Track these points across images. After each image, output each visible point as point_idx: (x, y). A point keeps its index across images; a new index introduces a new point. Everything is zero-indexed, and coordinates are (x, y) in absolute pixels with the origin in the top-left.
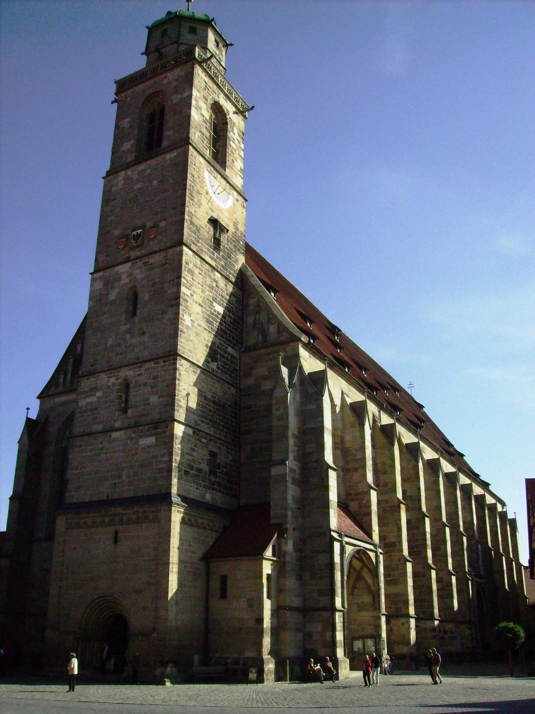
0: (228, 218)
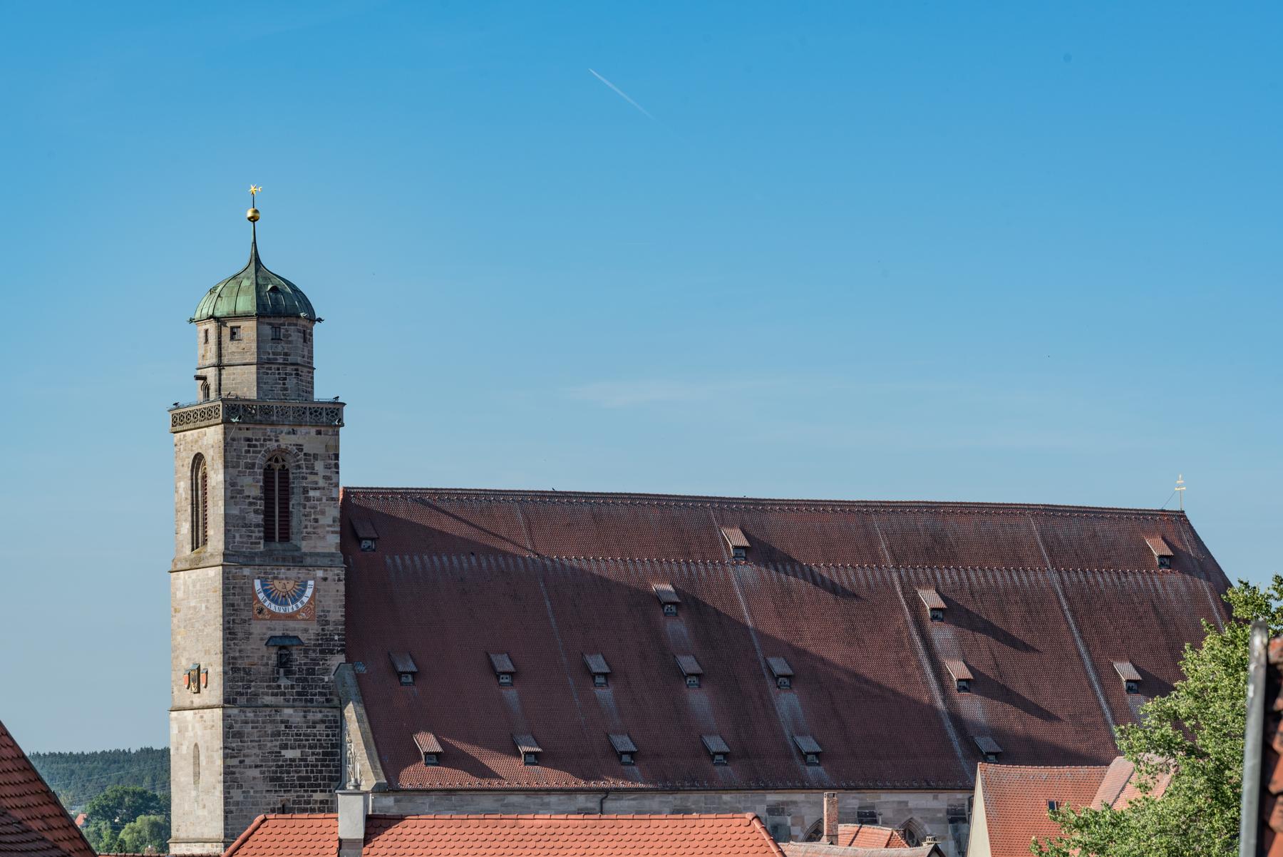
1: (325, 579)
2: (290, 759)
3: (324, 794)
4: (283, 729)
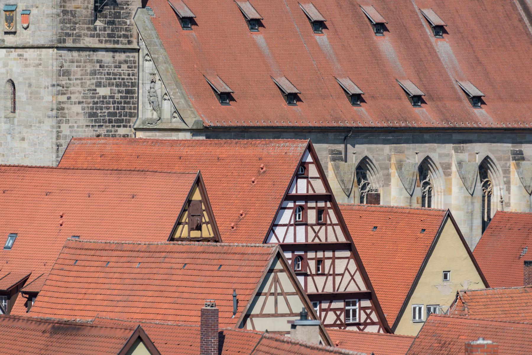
2: (103, 96)
3: (125, 129)
4: (98, 68)
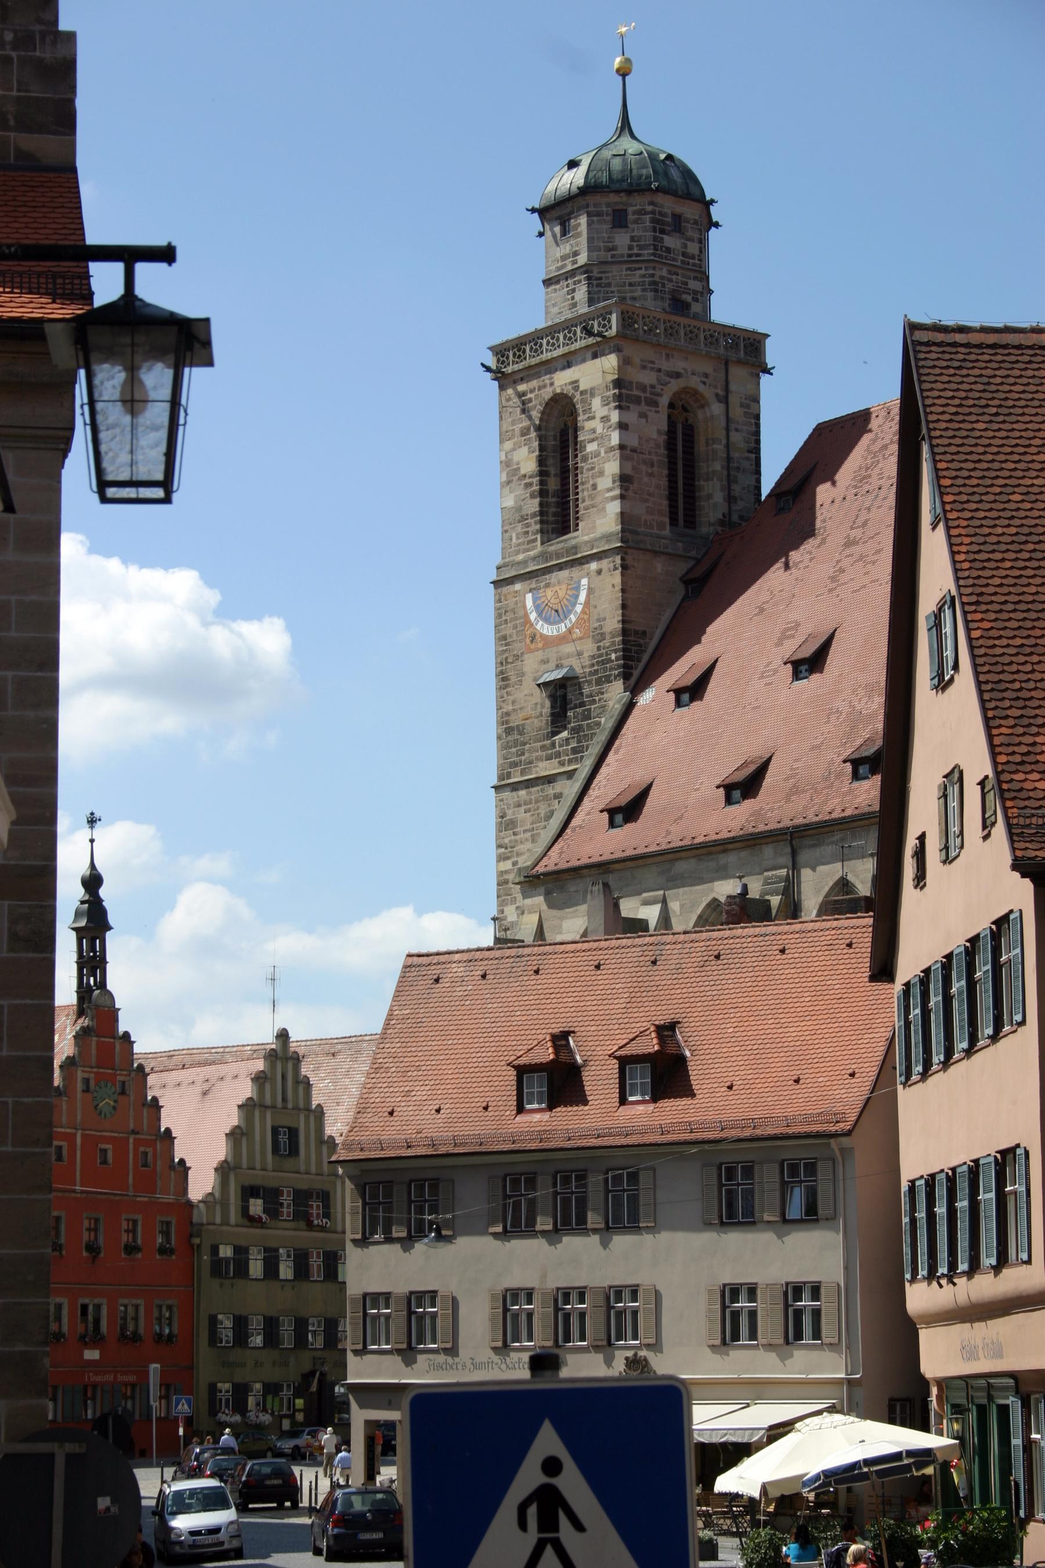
0: (581, 638)
1: (599, 572)
